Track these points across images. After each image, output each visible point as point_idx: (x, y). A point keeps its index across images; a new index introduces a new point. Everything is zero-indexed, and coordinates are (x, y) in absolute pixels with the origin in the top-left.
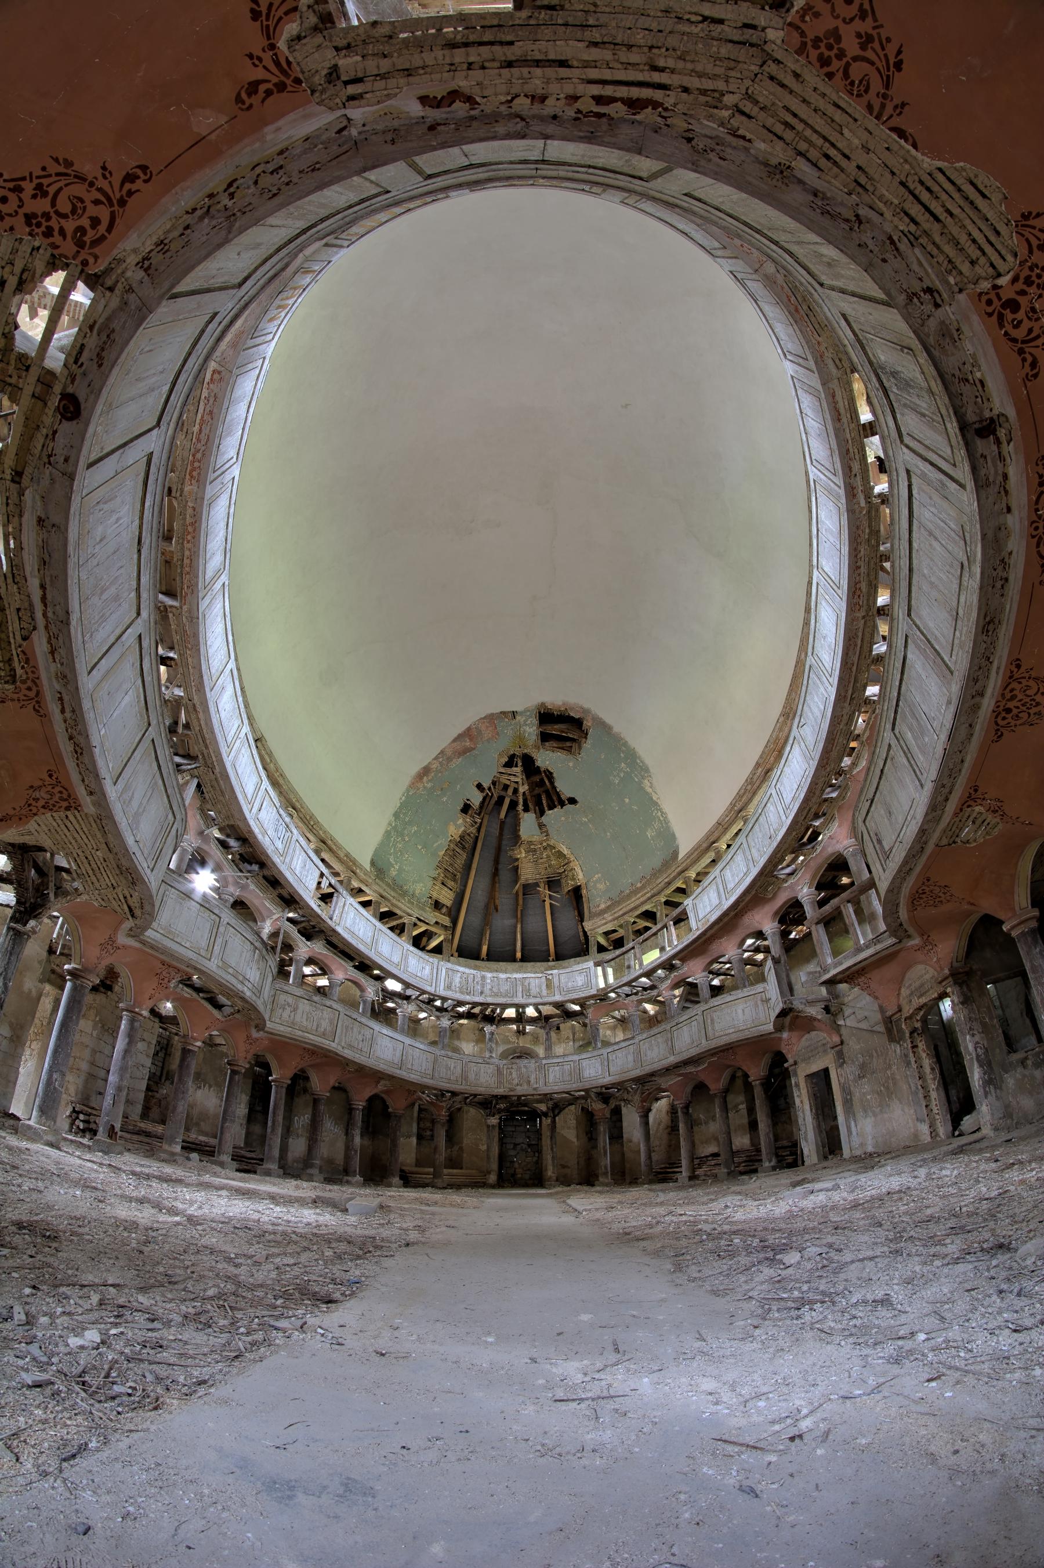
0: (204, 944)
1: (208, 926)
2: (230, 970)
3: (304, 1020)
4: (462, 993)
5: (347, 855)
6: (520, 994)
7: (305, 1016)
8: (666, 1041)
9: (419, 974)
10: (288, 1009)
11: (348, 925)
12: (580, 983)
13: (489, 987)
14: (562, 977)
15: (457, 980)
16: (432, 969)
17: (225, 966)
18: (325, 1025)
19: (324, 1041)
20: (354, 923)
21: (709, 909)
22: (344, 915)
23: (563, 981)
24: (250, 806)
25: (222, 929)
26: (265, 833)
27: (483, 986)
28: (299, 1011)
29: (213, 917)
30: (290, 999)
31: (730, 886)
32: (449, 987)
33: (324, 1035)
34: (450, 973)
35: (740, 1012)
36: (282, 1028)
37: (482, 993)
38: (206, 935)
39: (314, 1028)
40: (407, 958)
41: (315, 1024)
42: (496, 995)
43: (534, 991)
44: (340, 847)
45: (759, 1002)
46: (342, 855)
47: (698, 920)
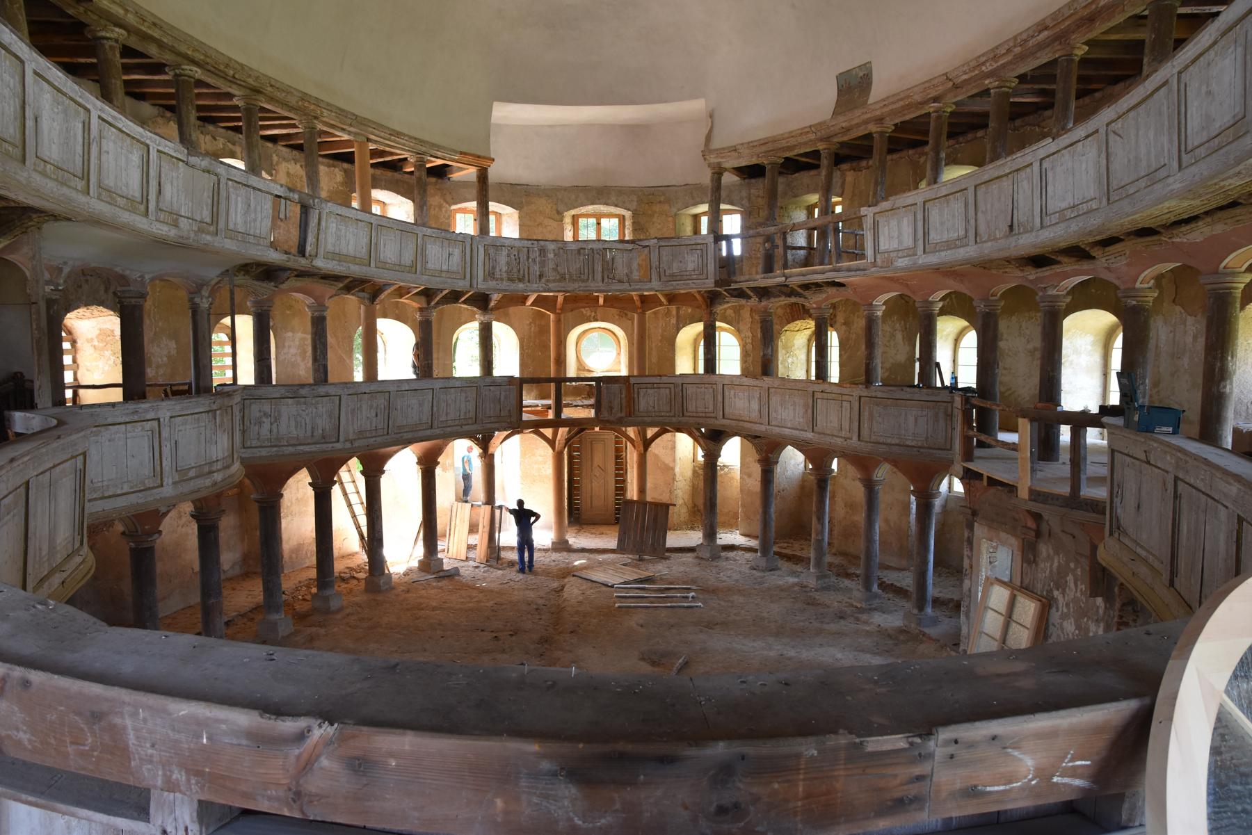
0: (147, 471)
1: (145, 443)
2: (192, 474)
3: (293, 429)
4: (511, 280)
5: (305, 97)
6: (599, 276)
7: (293, 424)
8: (806, 405)
9: (445, 268)
10: (267, 421)
11: (330, 248)
12: (690, 266)
13: (551, 265)
14: (664, 252)
15: (503, 260)
16: (464, 252)
17: (183, 475)
18: (323, 424)
19: (324, 447)
20: (338, 238)
21: (894, 245)
22: (322, 236)
23: (664, 259)
24: (142, 208)
25: (165, 434)
26: (175, 219)
27: (542, 264)
28: (284, 419)
29: (148, 425)
30: (267, 407)
31: (934, 236)
32: (491, 275)
33: (324, 439)
34: (492, 251)
35: (911, 420)
36: (264, 452)
37: (541, 276)
38: (147, 455)
39: (309, 434)
40: (424, 250)
41: (309, 427)
42: (563, 278)
43: (621, 270)
44: (288, 91)
45: (941, 415)
46: (293, 101)
47: (876, 250)
